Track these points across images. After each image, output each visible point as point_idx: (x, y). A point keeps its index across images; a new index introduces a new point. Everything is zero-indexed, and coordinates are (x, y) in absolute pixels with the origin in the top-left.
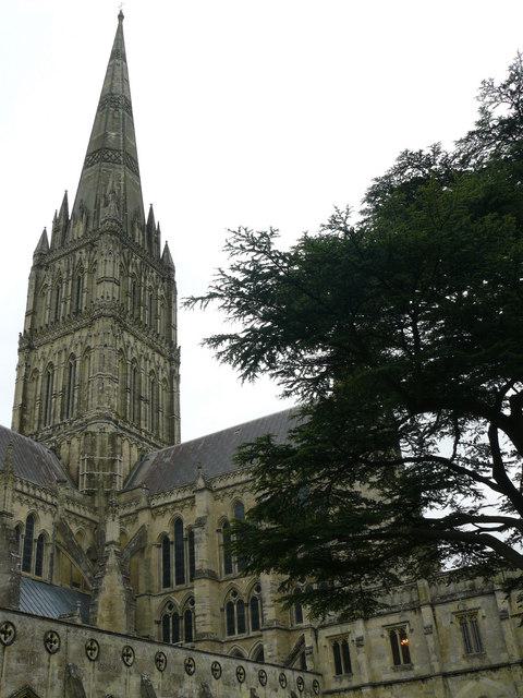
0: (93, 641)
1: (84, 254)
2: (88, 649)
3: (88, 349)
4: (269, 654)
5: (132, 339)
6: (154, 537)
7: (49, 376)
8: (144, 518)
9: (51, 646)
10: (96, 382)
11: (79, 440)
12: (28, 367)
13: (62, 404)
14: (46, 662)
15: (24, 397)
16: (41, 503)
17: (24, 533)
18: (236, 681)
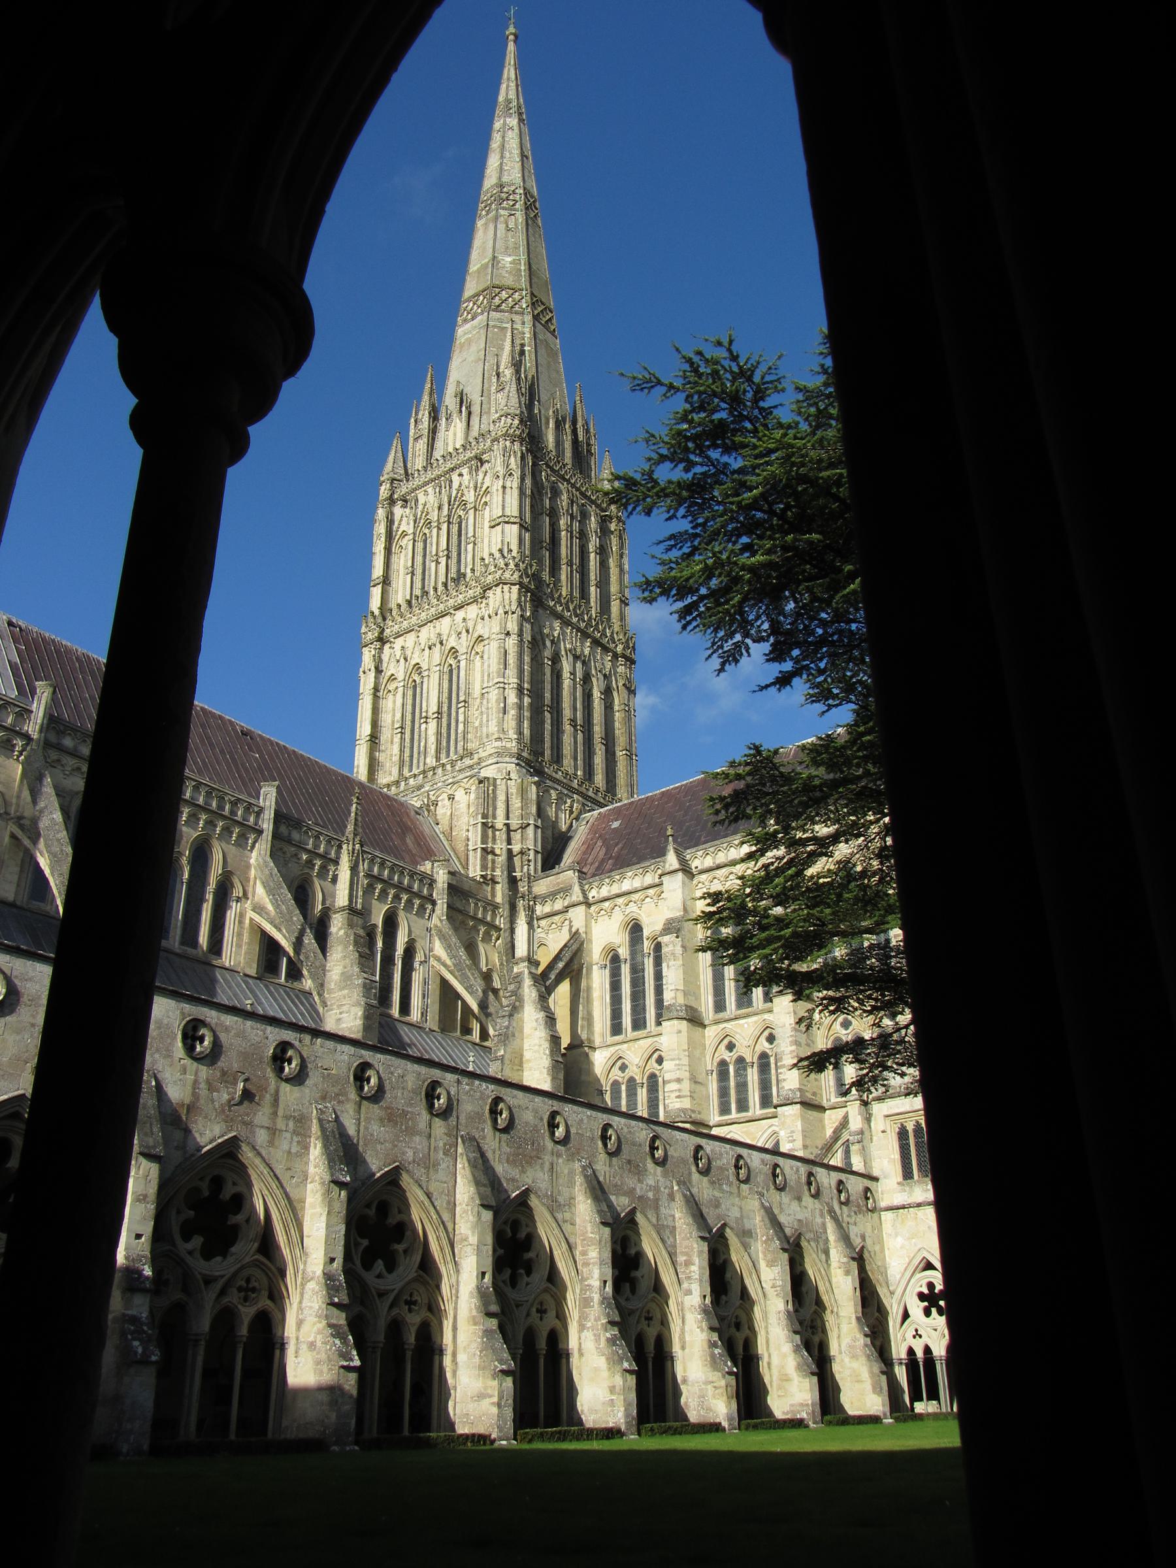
1: (466, 477)
6: (595, 953)
8: (578, 916)
10: (494, 695)
13: (439, 733)
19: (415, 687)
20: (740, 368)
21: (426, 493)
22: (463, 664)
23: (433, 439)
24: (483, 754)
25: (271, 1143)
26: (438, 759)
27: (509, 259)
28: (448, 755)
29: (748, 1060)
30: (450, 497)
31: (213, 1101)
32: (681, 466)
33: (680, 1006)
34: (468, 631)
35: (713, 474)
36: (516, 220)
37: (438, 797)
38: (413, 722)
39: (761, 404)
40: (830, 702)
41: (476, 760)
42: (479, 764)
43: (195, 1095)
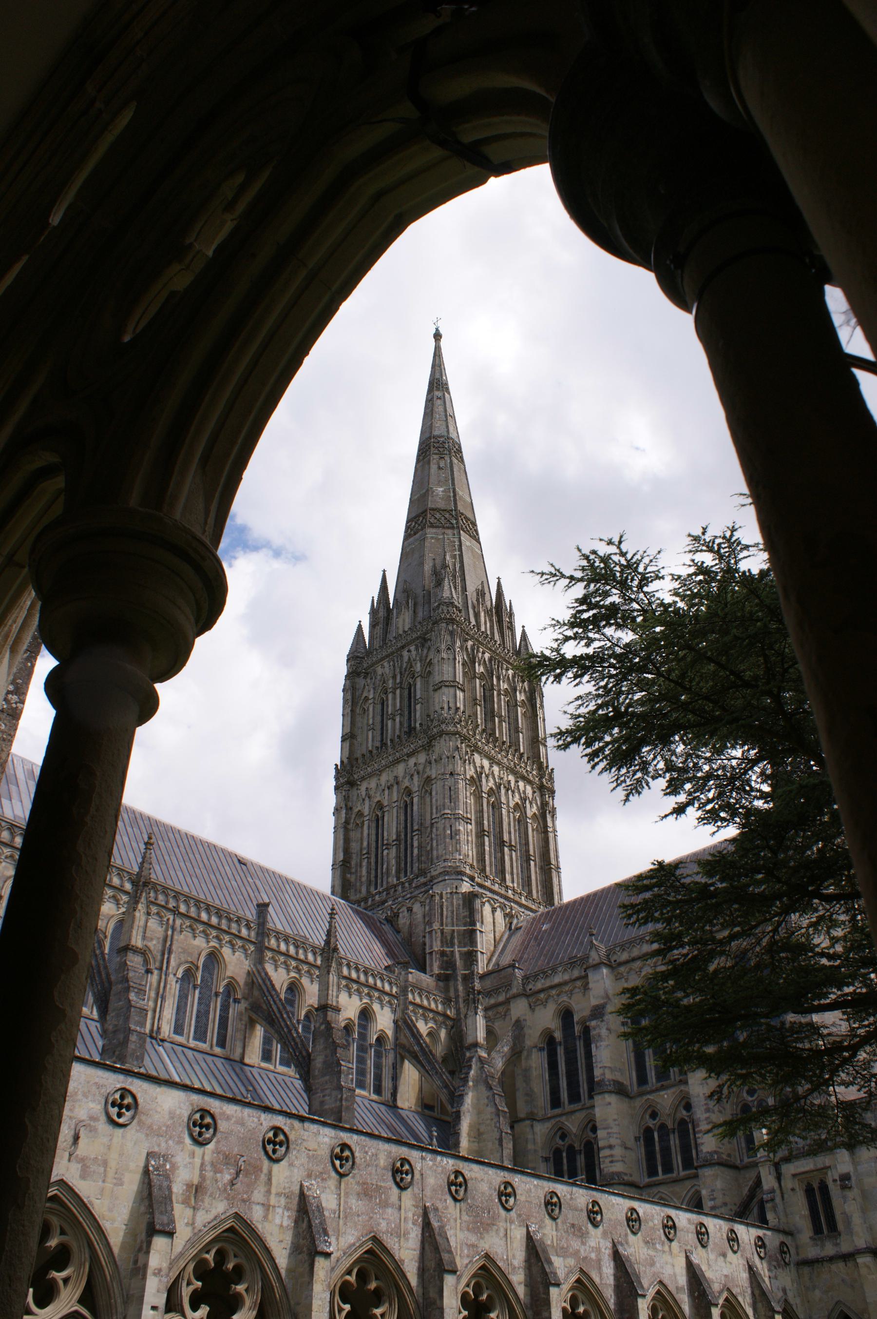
0: (458, 1173)
1: (414, 653)
2: (450, 1184)
3: (428, 780)
4: (710, 1204)
5: (486, 763)
6: (533, 1037)
7: (378, 821)
8: (519, 1008)
9: (402, 1179)
11: (423, 904)
12: (349, 809)
13: (398, 857)
14: (397, 1202)
15: (347, 851)
16: (376, 994)
17: (356, 1036)
18: (663, 1237)
19: (377, 820)
20: (628, 561)
21: (383, 667)
22: (415, 800)
23: (387, 624)
24: (434, 873)
25: (266, 1217)
26: (398, 878)
27: (441, 489)
28: (406, 875)
29: (670, 1126)
30: (401, 668)
31: (216, 1181)
32: (583, 642)
33: (609, 1081)
34: (418, 773)
35: (610, 647)
36: (446, 461)
37: (399, 909)
38: (377, 848)
39: (645, 589)
40: (719, 823)
41: (428, 878)
42: (431, 881)
43: (202, 1177)
